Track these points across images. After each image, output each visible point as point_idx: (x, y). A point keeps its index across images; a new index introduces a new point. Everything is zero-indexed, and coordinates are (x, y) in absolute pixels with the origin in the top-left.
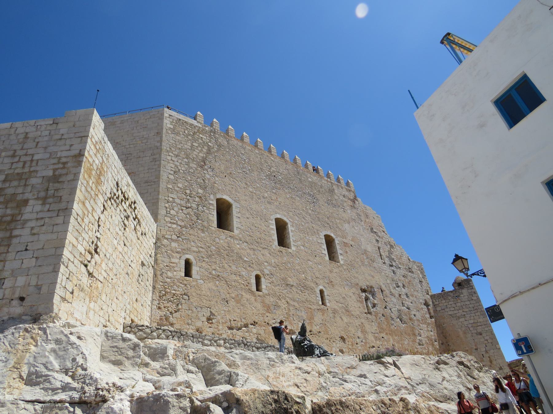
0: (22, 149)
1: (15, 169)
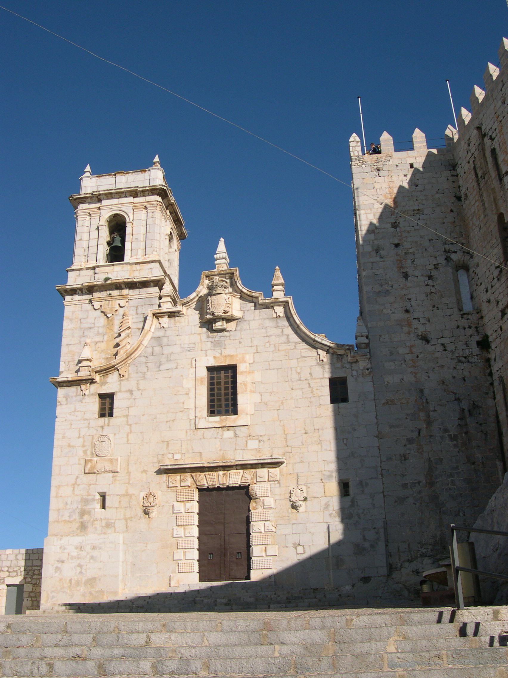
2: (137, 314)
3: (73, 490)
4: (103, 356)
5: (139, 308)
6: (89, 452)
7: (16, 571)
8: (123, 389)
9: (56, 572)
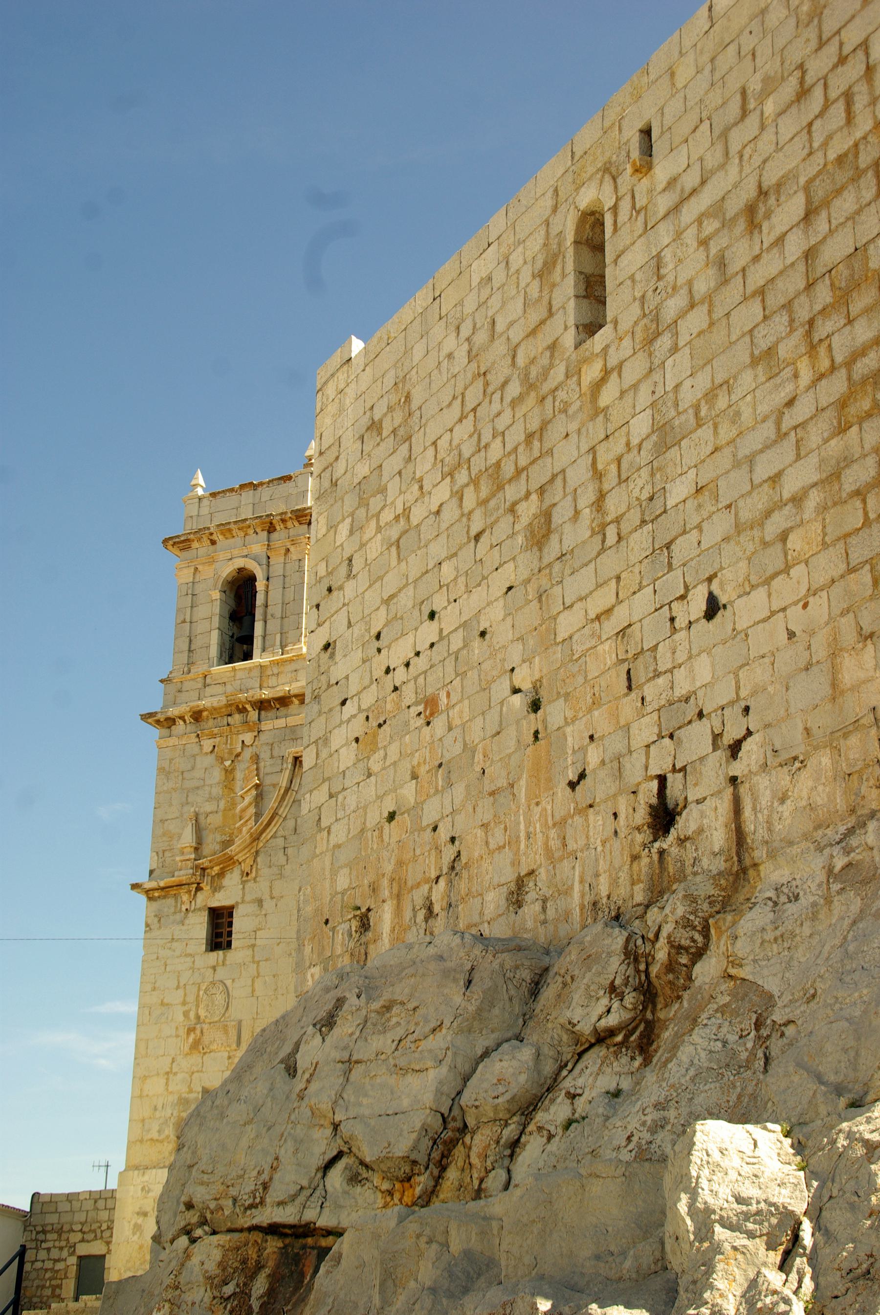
0: (822, 44)
1: (825, 145)
2: (272, 757)
3: (167, 1084)
4: (219, 838)
5: (275, 745)
6: (192, 1015)
7: (94, 1231)
8: (248, 898)
9: (134, 1234)
